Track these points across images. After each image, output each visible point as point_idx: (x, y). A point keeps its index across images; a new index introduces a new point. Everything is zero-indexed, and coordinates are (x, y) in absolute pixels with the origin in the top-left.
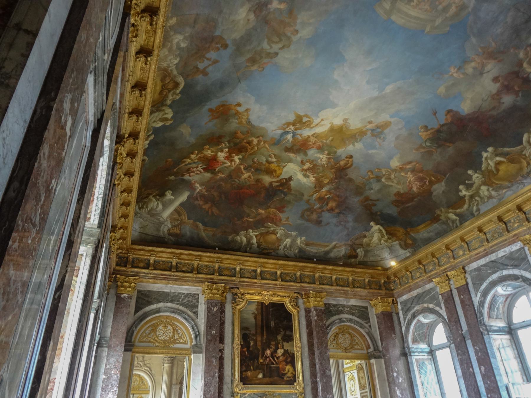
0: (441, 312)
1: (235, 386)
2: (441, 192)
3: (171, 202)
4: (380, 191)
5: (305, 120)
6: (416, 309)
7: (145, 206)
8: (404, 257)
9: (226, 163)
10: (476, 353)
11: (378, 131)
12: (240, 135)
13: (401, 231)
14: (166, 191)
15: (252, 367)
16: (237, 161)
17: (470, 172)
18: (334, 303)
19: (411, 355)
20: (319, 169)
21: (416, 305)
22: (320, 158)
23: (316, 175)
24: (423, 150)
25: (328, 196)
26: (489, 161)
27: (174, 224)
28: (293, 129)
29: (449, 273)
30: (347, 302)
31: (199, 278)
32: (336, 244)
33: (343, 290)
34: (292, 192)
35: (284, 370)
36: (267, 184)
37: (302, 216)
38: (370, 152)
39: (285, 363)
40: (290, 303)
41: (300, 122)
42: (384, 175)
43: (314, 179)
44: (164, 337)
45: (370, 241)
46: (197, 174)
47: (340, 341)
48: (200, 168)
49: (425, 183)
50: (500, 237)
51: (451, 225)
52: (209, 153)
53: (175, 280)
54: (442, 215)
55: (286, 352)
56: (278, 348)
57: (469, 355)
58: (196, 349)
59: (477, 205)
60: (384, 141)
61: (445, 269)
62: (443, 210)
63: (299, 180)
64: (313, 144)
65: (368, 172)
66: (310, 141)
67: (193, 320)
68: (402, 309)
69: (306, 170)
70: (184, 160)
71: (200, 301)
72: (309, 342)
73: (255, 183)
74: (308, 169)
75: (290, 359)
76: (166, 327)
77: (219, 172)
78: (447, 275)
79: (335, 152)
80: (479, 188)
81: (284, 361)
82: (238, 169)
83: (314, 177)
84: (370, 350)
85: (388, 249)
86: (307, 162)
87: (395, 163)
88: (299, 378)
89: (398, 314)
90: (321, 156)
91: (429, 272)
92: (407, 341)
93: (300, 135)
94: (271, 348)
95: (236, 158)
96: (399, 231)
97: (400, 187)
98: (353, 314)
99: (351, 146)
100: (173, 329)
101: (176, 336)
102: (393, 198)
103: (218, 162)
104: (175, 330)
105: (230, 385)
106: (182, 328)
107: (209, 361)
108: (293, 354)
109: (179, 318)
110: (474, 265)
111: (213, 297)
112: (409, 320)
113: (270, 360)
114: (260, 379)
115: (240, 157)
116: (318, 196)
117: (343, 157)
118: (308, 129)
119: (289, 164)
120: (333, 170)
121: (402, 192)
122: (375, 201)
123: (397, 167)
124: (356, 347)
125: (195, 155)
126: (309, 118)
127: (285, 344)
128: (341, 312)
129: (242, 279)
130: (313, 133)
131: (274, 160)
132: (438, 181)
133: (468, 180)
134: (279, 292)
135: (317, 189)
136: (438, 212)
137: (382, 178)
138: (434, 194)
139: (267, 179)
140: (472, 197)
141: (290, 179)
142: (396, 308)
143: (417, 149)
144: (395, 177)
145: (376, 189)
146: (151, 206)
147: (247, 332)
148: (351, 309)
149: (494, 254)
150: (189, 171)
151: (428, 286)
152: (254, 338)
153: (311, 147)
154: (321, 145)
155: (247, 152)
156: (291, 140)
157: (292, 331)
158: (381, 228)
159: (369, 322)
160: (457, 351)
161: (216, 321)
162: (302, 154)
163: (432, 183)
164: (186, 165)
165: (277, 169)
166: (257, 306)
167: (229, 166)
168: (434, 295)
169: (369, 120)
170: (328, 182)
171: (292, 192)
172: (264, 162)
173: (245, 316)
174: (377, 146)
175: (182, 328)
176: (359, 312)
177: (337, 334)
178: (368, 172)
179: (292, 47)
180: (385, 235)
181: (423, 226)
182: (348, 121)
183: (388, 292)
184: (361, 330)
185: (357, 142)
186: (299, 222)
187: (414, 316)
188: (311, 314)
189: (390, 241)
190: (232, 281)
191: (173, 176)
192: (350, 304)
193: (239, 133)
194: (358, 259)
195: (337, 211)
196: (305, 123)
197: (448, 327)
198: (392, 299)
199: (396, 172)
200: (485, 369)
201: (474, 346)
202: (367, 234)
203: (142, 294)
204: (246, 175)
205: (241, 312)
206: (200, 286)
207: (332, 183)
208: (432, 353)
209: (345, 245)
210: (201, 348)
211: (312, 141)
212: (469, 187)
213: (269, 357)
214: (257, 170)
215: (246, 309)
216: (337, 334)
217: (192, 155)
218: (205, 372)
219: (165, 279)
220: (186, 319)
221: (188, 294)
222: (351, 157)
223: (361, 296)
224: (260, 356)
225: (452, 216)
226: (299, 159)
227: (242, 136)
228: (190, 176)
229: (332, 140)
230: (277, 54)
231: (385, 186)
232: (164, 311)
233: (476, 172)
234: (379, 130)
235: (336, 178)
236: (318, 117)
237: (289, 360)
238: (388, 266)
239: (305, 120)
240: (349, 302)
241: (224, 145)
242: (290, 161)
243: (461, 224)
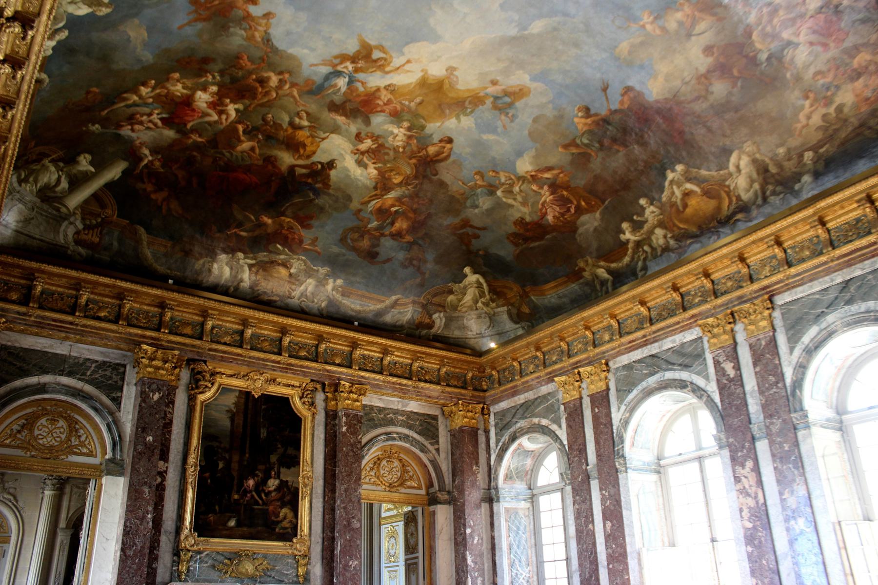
0: (559, 432)
1: (182, 537)
2: (592, 229)
3: (86, 178)
4: (490, 212)
5: (376, 54)
6: (518, 425)
7: (31, 179)
8: (513, 336)
9: (208, 115)
10: (603, 500)
11: (506, 102)
12: (245, 62)
13: (515, 289)
14: (79, 154)
15: (217, 507)
16: (233, 114)
17: (643, 202)
18: (381, 405)
19: (498, 501)
20: (387, 154)
21: (520, 419)
22: (392, 133)
23: (380, 165)
24: (574, 150)
25: (396, 208)
26: (675, 187)
27: (88, 223)
28: (350, 69)
29: (581, 370)
30: (403, 406)
31: (130, 334)
32: (398, 300)
33: (400, 384)
34: (331, 191)
35: (278, 515)
36: (284, 168)
37: (343, 240)
38: (485, 137)
39: (279, 503)
40: (301, 398)
41: (365, 57)
42: (503, 184)
43: (375, 172)
44: (49, 439)
45: (460, 301)
46: (148, 128)
47: (382, 472)
48: (155, 117)
49: (568, 210)
50: (672, 316)
51: (598, 287)
52: (178, 89)
53: (82, 333)
54: (587, 269)
55: (283, 485)
56: (270, 477)
57: (591, 504)
58: (114, 467)
59: (645, 259)
60: (512, 121)
61: (577, 363)
62: (590, 261)
63: (346, 169)
64: (385, 104)
65: (476, 174)
66: (379, 98)
67: (112, 414)
68: (496, 425)
69: (363, 153)
70: (125, 95)
71: (126, 378)
72: (325, 469)
73: (260, 163)
74: (367, 152)
75: (290, 497)
76: (53, 421)
77: (193, 130)
78: (579, 373)
79: (423, 128)
80: (651, 232)
81: (278, 500)
82: (232, 129)
83: (375, 168)
84: (432, 490)
85: (488, 319)
86: (368, 137)
87: (524, 166)
88: (302, 531)
89: (487, 432)
90: (396, 131)
91: (550, 365)
92: (496, 478)
93: (362, 83)
94: (257, 476)
95: (232, 109)
96: (511, 289)
97: (525, 210)
98: (410, 427)
100: (70, 426)
101: (73, 439)
102: (512, 229)
103: (193, 110)
104: (73, 427)
105: (172, 537)
106: (88, 426)
107: (136, 491)
108: (297, 490)
109: (84, 406)
110: (625, 360)
111: (155, 373)
112: (504, 444)
113: (252, 496)
114: (232, 528)
115: (240, 106)
116: (378, 205)
117: (436, 138)
118: (379, 73)
119: (333, 135)
120: (414, 161)
121: (528, 219)
122: (479, 229)
124: (408, 483)
125: (149, 90)
126: (384, 52)
127: (283, 470)
128: (391, 423)
129: (214, 346)
130: (387, 83)
131: (305, 123)
132: (590, 210)
133: (639, 215)
134: (282, 377)
135: (378, 192)
136: (582, 264)
137: (498, 189)
138: (581, 230)
139: (286, 159)
140: (638, 244)
141: (331, 165)
142: (486, 422)
143: (566, 147)
144: (521, 191)
145: (485, 207)
146: (46, 180)
147: (215, 444)
148: (409, 417)
149: (656, 344)
150: (131, 119)
151: (545, 389)
152: (227, 456)
153: (379, 109)
154: (399, 108)
155: (254, 98)
156: (344, 89)
157: (297, 447)
158: (482, 280)
159: (437, 442)
160: (573, 497)
161: (154, 419)
162: (359, 120)
163: (579, 211)
164: (128, 106)
165: (308, 142)
166: (238, 397)
167: (216, 122)
168: (552, 405)
169: (492, 77)
170: (401, 182)
171: (331, 191)
172: (285, 125)
173: (214, 414)
174: (500, 130)
175: (88, 426)
176: (421, 425)
177: (379, 459)
178: (476, 174)
180: (487, 293)
181: (552, 284)
182: (455, 73)
183: (476, 393)
184: (421, 455)
185: (466, 115)
186: (335, 249)
187: (513, 438)
188: (337, 422)
189: (494, 305)
190: (193, 346)
191: (97, 126)
192: (408, 409)
193: (246, 57)
194: (433, 331)
195: (408, 238)
196: (376, 61)
197: (566, 458)
198: (481, 405)
199: (523, 182)
200: (613, 525)
201: (601, 489)
202: (456, 287)
203: (10, 353)
204: (246, 145)
205: (206, 405)
206: (129, 350)
207: (407, 184)
208: (533, 499)
209: (414, 302)
210: (122, 466)
211: (383, 97)
212: (637, 226)
213: (251, 492)
214: (269, 137)
215: (216, 402)
216: (379, 459)
217: (142, 88)
218: (127, 511)
219: (60, 329)
220: (96, 410)
221: (104, 363)
222: (450, 141)
223: (429, 397)
224: (235, 488)
225: (602, 273)
226: (353, 128)
227: (249, 66)
228: (133, 130)
229: (420, 103)
231: (500, 205)
232: (54, 391)
233: (652, 204)
234: (507, 100)
235: (416, 177)
236: (403, 54)
237: (287, 498)
238: (485, 349)
239: (376, 54)
240: (407, 405)
241: (210, 78)
242: (335, 129)
243: (615, 288)
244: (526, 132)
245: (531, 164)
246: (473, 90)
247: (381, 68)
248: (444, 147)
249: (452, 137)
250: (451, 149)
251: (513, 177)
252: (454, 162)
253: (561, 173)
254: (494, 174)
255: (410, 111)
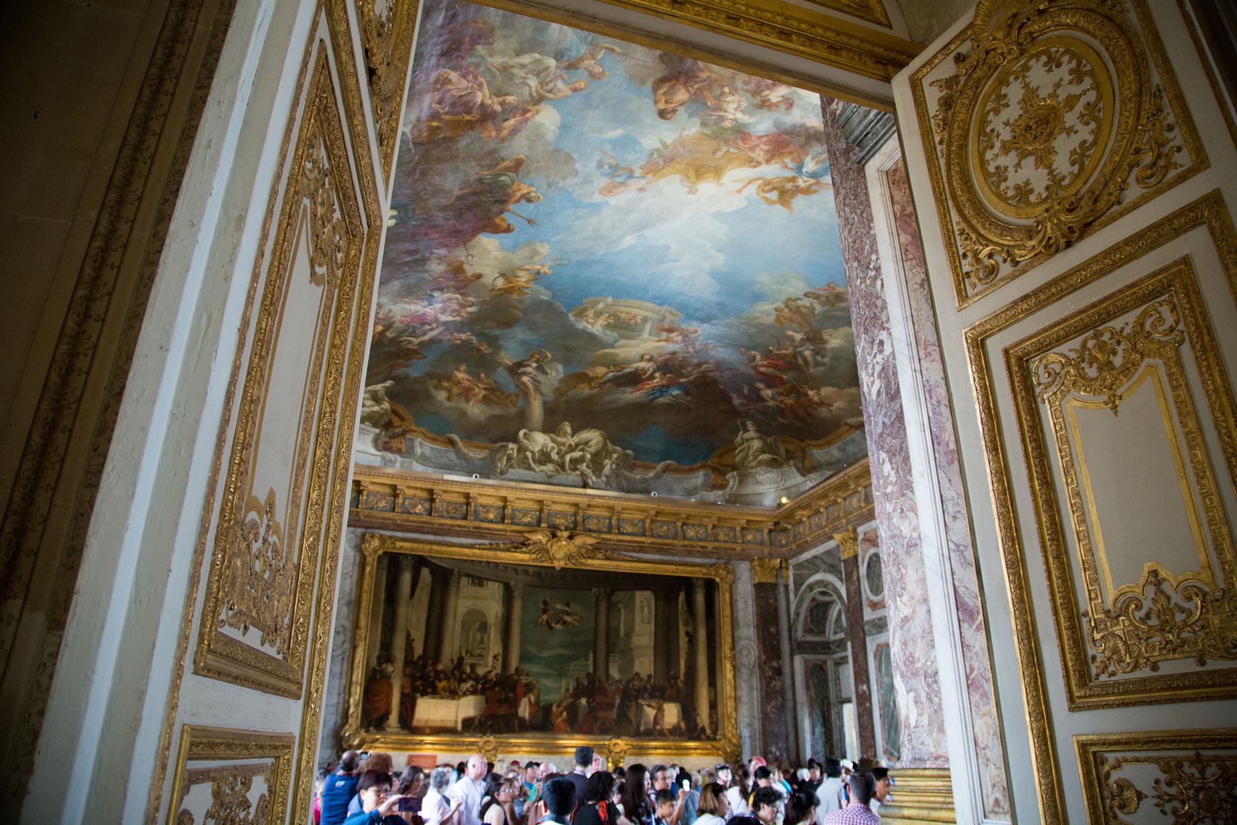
5: (774, 195)
11: (619, 174)
64: (757, 146)
65: (603, 73)
79: (704, 124)
87: (547, 118)
90: (739, 115)
97: (498, 60)
99: (669, 141)
117: (682, 113)
123: (538, 112)
137: (557, 67)
153: (764, 139)
154: (740, 143)
156: (808, 159)
174: (608, 147)
179: (784, 297)
185: (657, 150)
196: (774, 189)
211: (762, 153)
222: (662, 114)
229: (715, 152)
230: (806, 295)
244: (575, 156)
245: (540, 125)
246: (661, 177)
247: (767, 183)
248: (666, 102)
249: (661, 121)
250: (656, 102)
251: (550, 95)
252: (643, 83)
253: (497, 136)
254: (577, 85)
255: (726, 141)
